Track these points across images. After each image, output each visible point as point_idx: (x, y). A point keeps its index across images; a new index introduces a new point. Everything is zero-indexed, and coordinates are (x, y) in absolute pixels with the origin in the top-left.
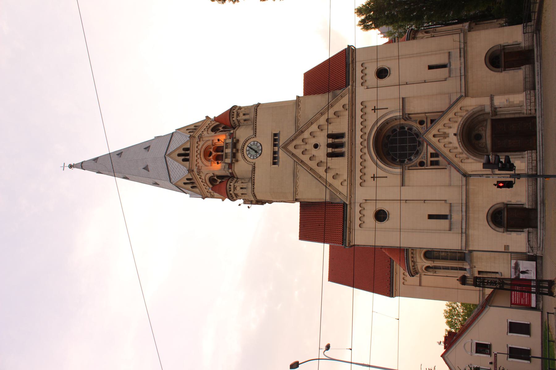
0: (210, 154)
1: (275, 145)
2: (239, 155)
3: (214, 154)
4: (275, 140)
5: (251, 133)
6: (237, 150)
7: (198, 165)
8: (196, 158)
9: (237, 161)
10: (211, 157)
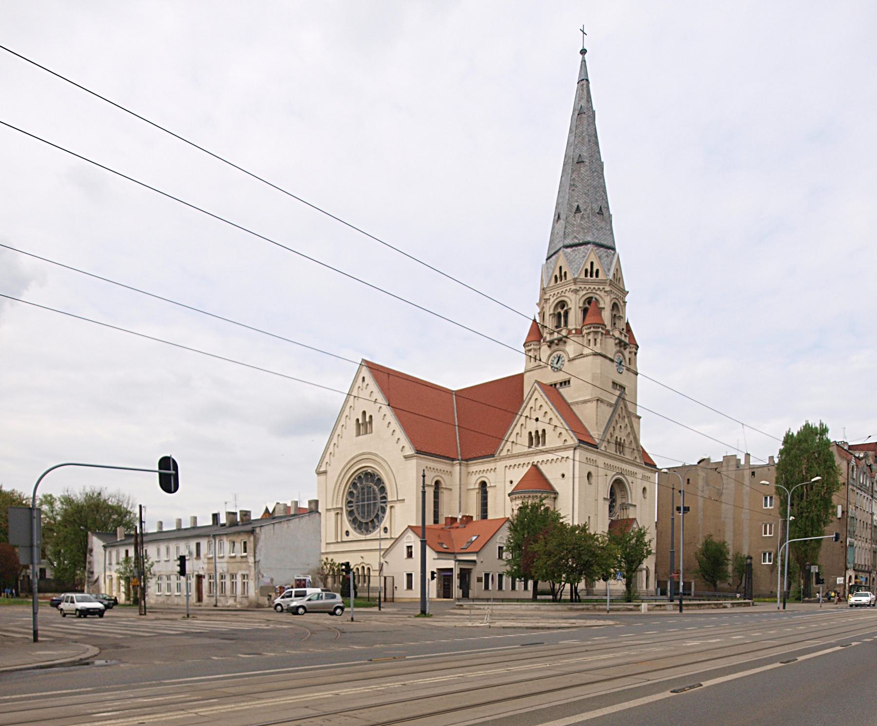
0: (562, 308)
1: (561, 384)
2: (554, 347)
3: (562, 313)
4: (565, 382)
5: (571, 356)
6: (557, 345)
7: (551, 297)
8: (556, 293)
9: (549, 347)
10: (559, 310)
